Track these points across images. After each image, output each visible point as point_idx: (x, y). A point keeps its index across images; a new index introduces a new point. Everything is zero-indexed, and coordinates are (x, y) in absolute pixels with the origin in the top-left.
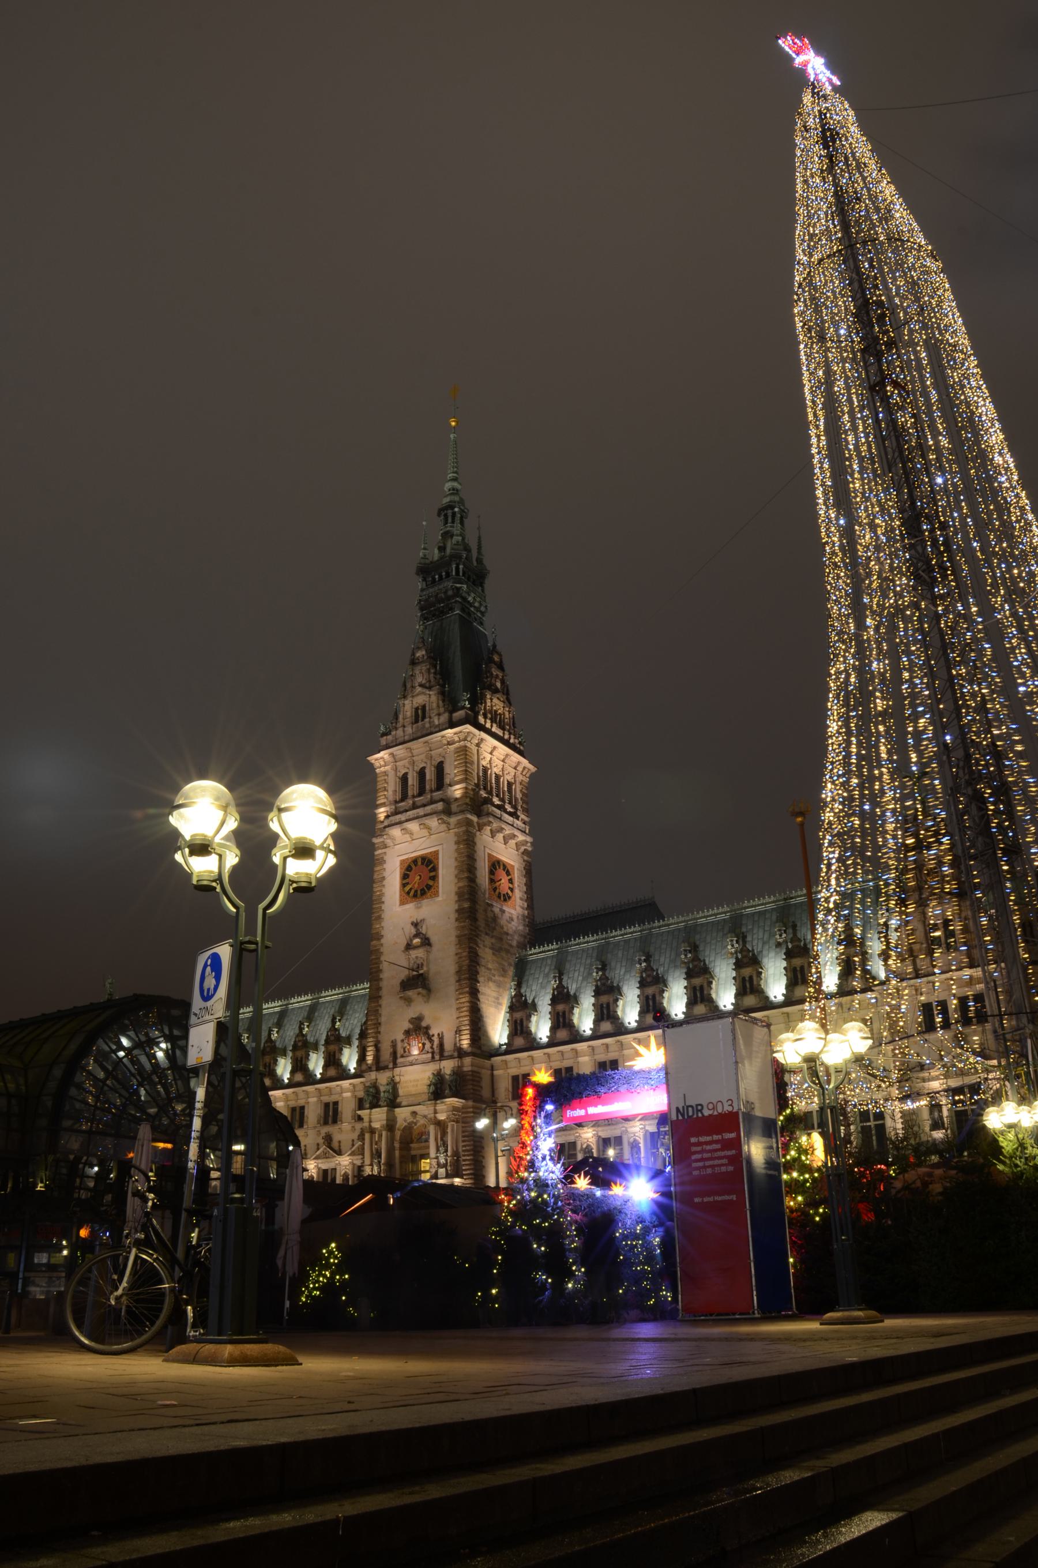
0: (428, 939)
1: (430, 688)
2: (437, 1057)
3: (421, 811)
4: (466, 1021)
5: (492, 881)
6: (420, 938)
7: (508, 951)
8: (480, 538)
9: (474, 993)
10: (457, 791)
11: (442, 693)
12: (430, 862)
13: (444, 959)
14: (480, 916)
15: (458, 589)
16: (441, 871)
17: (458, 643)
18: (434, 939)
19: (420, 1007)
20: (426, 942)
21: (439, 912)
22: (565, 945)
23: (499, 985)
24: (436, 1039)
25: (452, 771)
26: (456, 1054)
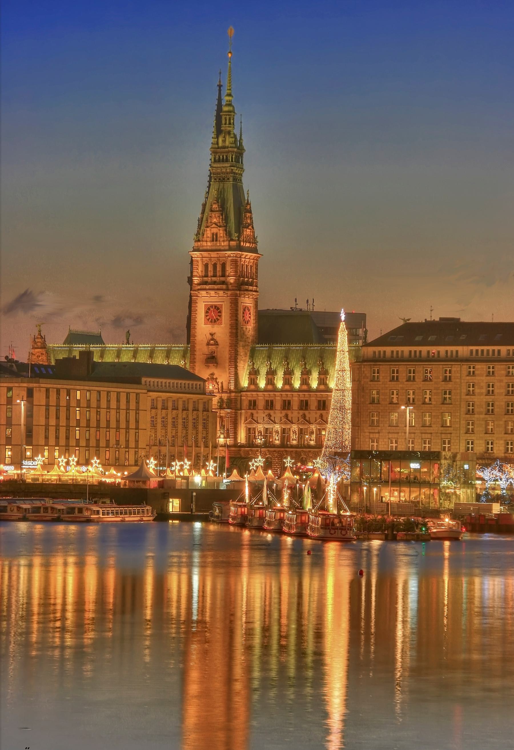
0: (217, 342)
1: (220, 227)
2: (221, 392)
3: (216, 287)
4: (233, 379)
5: (243, 317)
6: (213, 341)
7: (248, 345)
8: (241, 131)
9: (236, 367)
10: (231, 280)
11: (226, 230)
12: (218, 309)
13: (224, 351)
14: (239, 334)
15: (232, 170)
16: (223, 314)
17: (232, 201)
18: (219, 342)
19: (212, 370)
20: (216, 344)
21: (221, 331)
22: (272, 346)
23: (244, 361)
24: (220, 384)
25: (229, 270)
26: (228, 392)
